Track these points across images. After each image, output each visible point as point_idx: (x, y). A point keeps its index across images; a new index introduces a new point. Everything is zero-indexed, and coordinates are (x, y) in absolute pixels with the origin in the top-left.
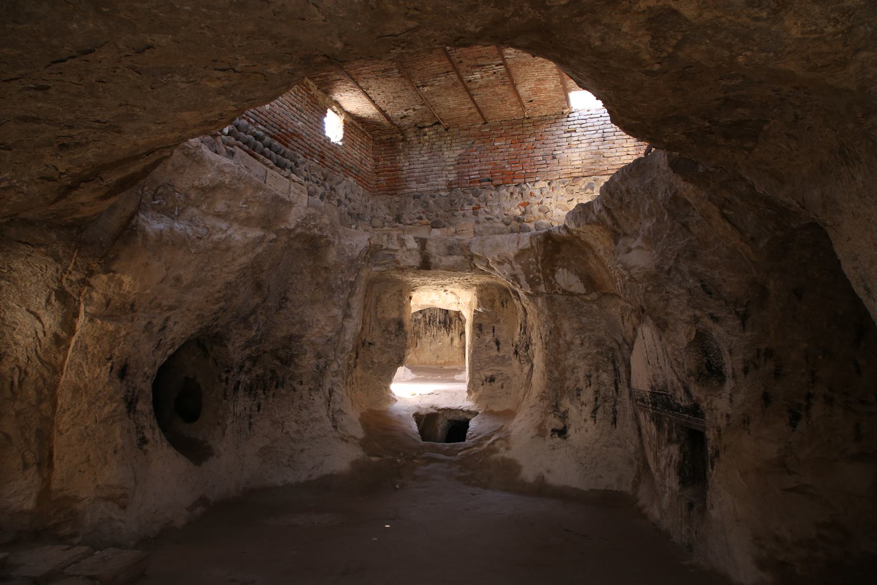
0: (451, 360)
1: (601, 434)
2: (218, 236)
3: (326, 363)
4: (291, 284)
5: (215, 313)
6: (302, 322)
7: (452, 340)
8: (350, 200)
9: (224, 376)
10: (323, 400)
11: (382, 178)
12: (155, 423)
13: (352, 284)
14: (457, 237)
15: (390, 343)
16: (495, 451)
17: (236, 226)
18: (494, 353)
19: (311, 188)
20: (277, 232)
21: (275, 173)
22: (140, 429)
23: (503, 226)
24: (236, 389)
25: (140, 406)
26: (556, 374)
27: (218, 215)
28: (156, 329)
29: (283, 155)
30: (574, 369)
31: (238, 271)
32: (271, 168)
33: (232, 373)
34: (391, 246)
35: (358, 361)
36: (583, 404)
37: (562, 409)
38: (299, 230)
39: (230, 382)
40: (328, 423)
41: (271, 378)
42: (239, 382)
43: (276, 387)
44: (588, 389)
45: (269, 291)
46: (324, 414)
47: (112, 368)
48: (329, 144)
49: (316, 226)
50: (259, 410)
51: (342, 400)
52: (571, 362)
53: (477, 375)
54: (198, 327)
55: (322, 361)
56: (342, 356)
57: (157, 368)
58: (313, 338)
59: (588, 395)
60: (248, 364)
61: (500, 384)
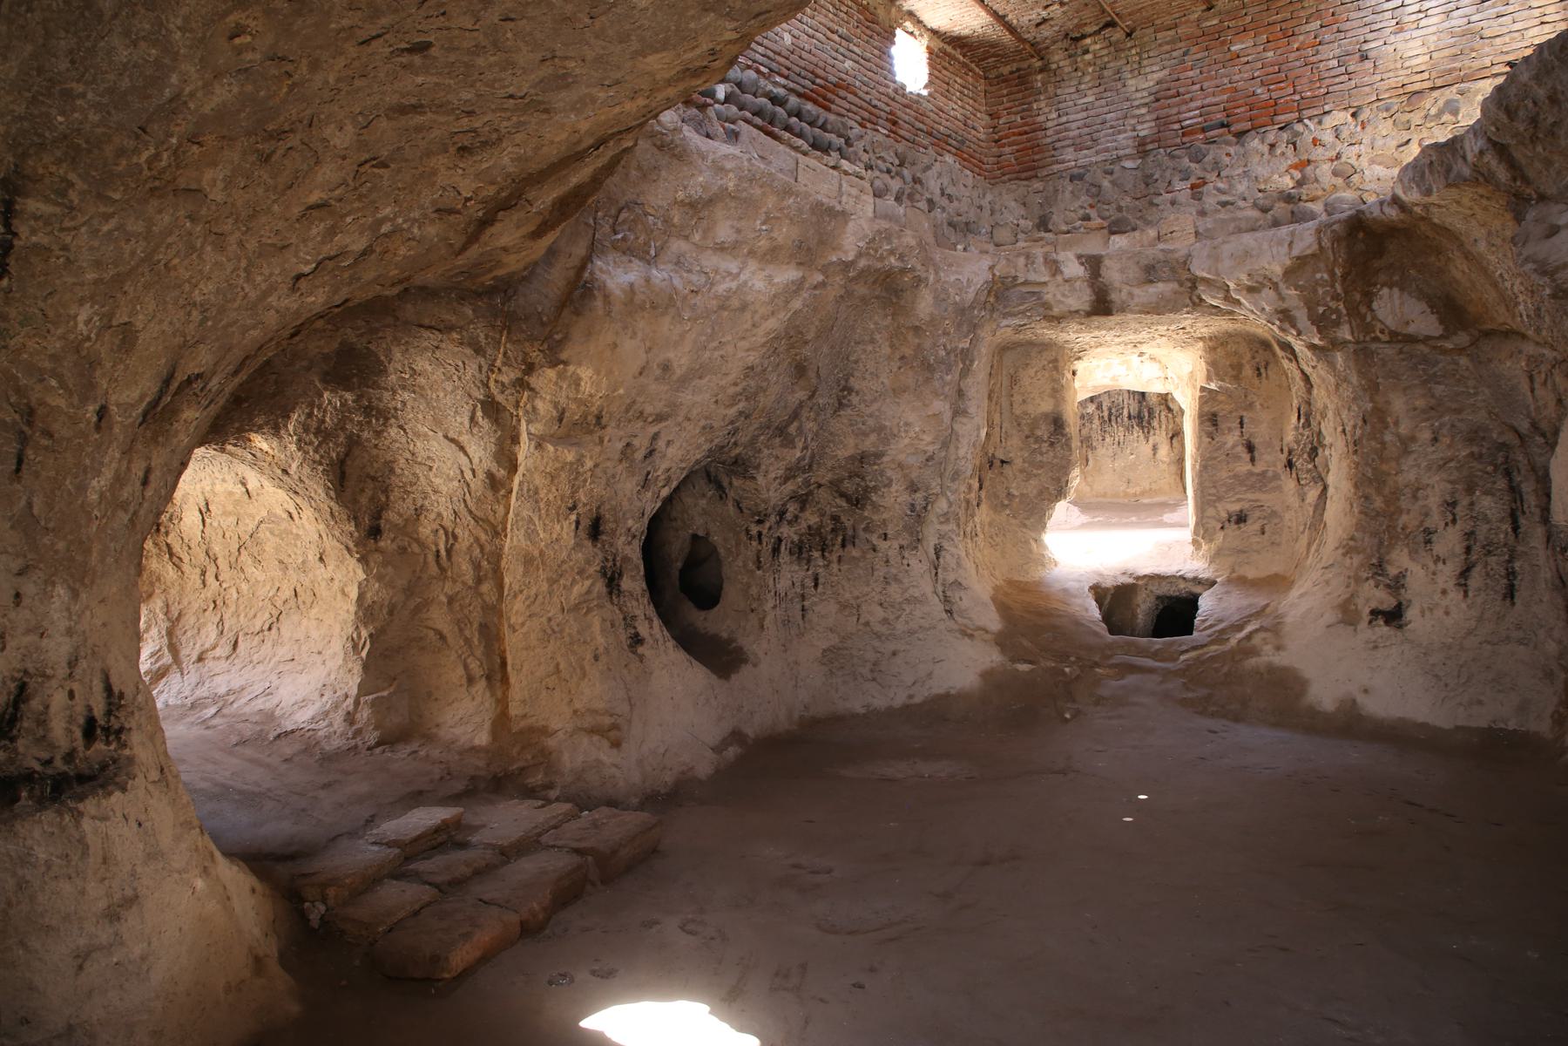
0: (1154, 486)
3: (926, 499)
4: (856, 362)
5: (732, 422)
6: (880, 429)
7: (1155, 448)
8: (950, 197)
9: (754, 530)
10: (925, 566)
11: (1007, 150)
12: (651, 611)
13: (966, 356)
14: (1161, 246)
15: (1039, 458)
16: (1254, 652)
17: (753, 265)
18: (1244, 467)
19: (878, 183)
20: (824, 270)
21: (813, 162)
22: (629, 620)
23: (1255, 213)
24: (776, 551)
25: (626, 584)
26: (1378, 503)
27: (721, 248)
28: (639, 455)
29: (823, 127)
30: (1416, 490)
31: (763, 345)
32: (805, 154)
33: (767, 525)
34: (1032, 277)
35: (983, 494)
36: (1437, 559)
37: (1392, 571)
38: (862, 263)
39: (765, 540)
40: (937, 607)
41: (833, 530)
42: (780, 540)
43: (843, 546)
44: (1450, 529)
45: (818, 376)
46: (928, 589)
47: (578, 523)
48: (904, 95)
49: (892, 252)
50: (816, 586)
51: (959, 564)
52: (1411, 476)
53: (1211, 512)
54: (706, 447)
55: (919, 496)
56: (954, 486)
57: (646, 520)
58: (901, 457)
59: (1449, 541)
60: (792, 508)
61: (1257, 526)
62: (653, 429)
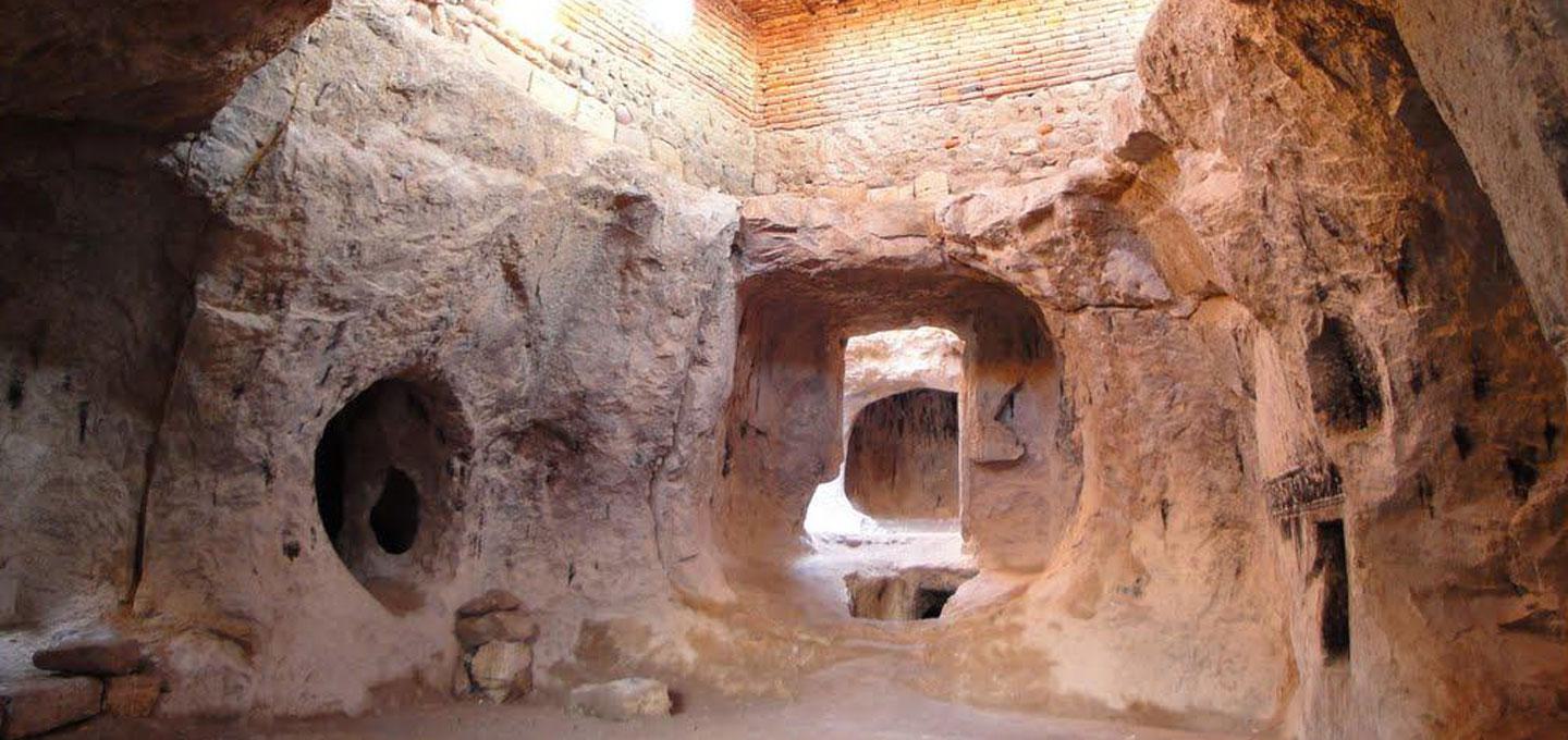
1: (1215, 596)
2: (430, 177)
9: (457, 464)
17: (466, 163)
62: (337, 318)
